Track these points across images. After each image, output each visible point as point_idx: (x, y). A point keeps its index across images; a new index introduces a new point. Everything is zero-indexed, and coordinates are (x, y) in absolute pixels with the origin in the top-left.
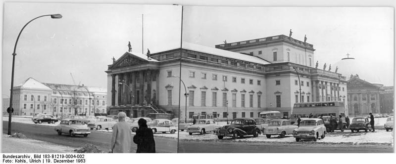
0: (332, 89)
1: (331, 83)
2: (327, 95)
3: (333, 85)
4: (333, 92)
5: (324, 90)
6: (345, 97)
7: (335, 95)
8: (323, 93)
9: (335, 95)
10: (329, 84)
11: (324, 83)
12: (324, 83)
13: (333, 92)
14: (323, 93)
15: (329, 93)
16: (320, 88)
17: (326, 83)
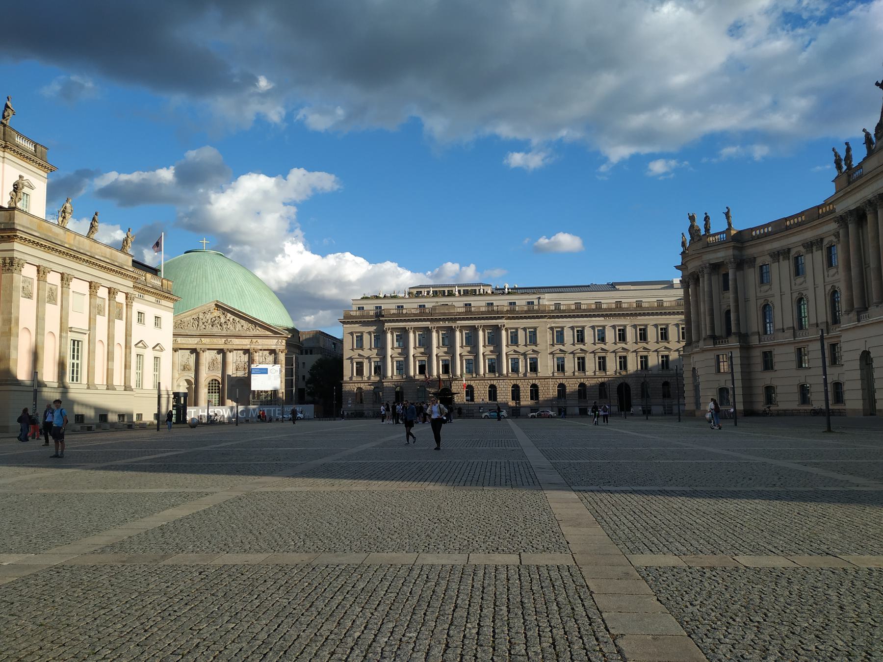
0: (95, 310)
1: (93, 287)
2: (64, 327)
3: (103, 293)
4: (102, 322)
5: (52, 312)
6: (162, 350)
7: (110, 337)
8: (40, 319)
9: (110, 337)
10: (79, 287)
11: (54, 279)
12: (54, 279)
13: (102, 322)
14: (40, 319)
15: (78, 320)
16: (29, 296)
17: (65, 279)
